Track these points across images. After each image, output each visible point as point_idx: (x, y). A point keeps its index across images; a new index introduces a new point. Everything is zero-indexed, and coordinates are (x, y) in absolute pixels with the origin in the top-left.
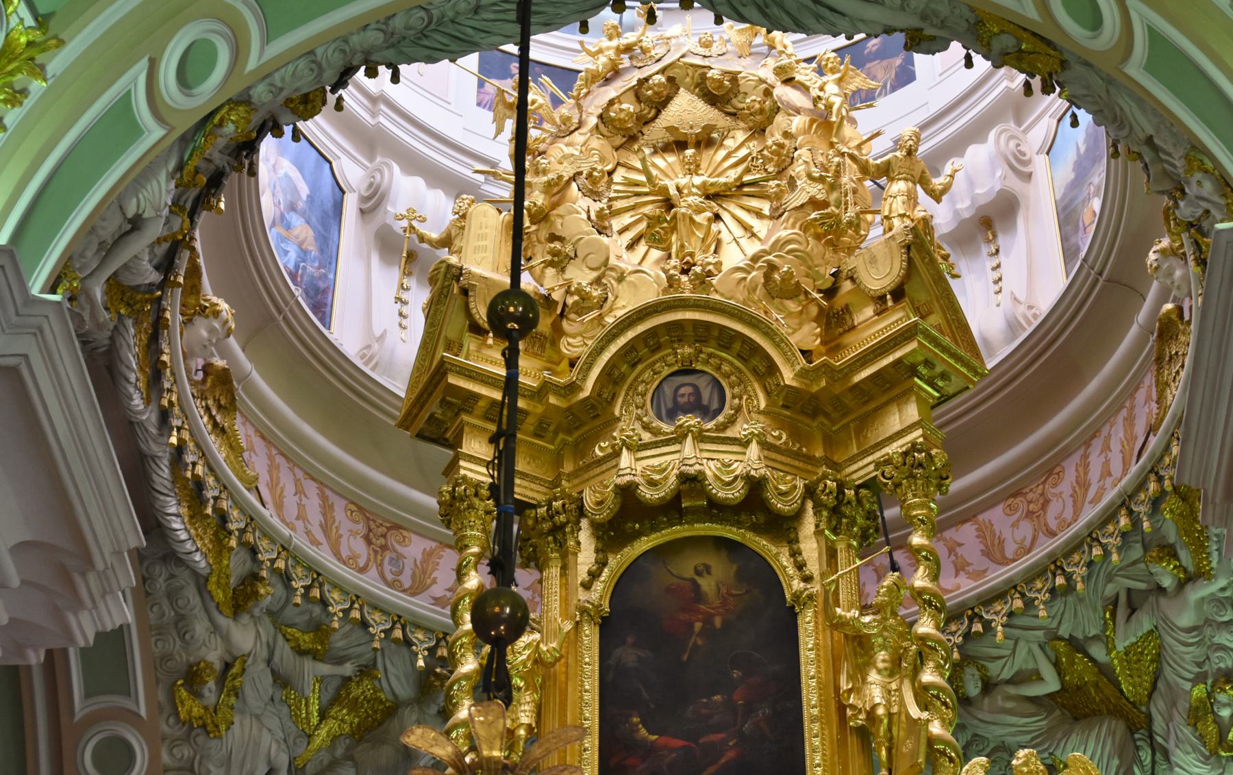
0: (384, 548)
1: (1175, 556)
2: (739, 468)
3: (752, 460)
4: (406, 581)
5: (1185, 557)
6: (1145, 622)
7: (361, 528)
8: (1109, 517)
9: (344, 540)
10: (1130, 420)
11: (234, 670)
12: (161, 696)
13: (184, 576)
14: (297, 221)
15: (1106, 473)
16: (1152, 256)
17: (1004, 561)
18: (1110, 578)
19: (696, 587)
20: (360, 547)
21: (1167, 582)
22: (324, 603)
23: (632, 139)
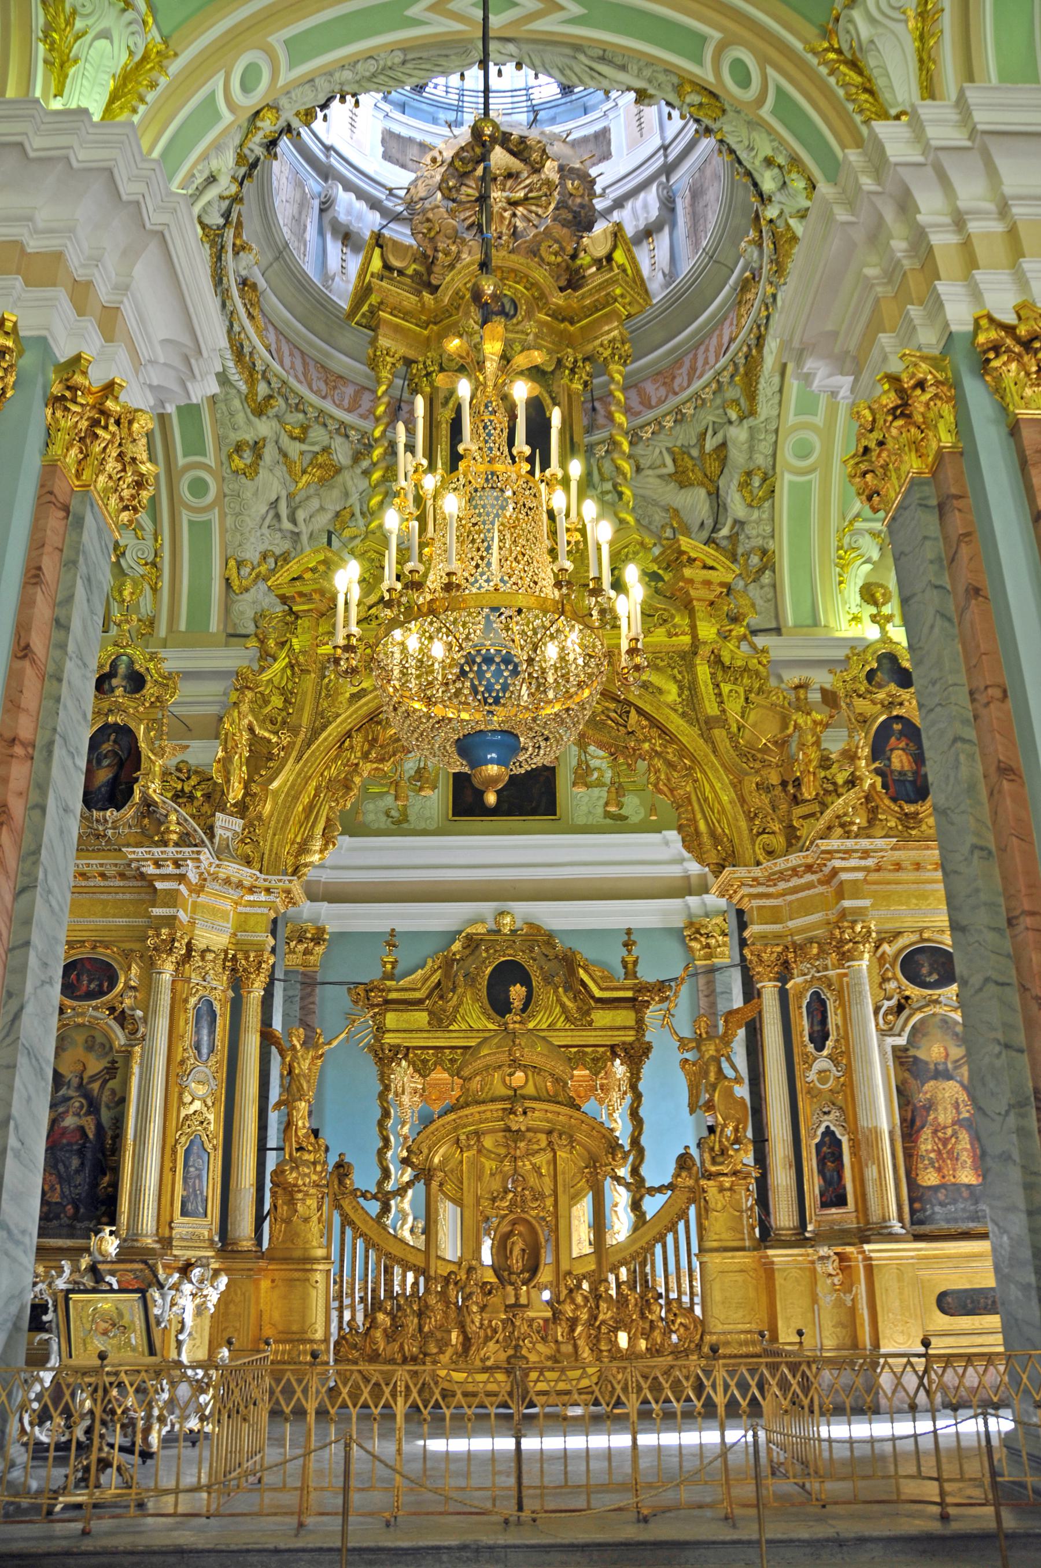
0: (335, 388)
10: (721, 336)
15: (706, 362)
16: (743, 244)
17: (650, 407)
20: (323, 386)
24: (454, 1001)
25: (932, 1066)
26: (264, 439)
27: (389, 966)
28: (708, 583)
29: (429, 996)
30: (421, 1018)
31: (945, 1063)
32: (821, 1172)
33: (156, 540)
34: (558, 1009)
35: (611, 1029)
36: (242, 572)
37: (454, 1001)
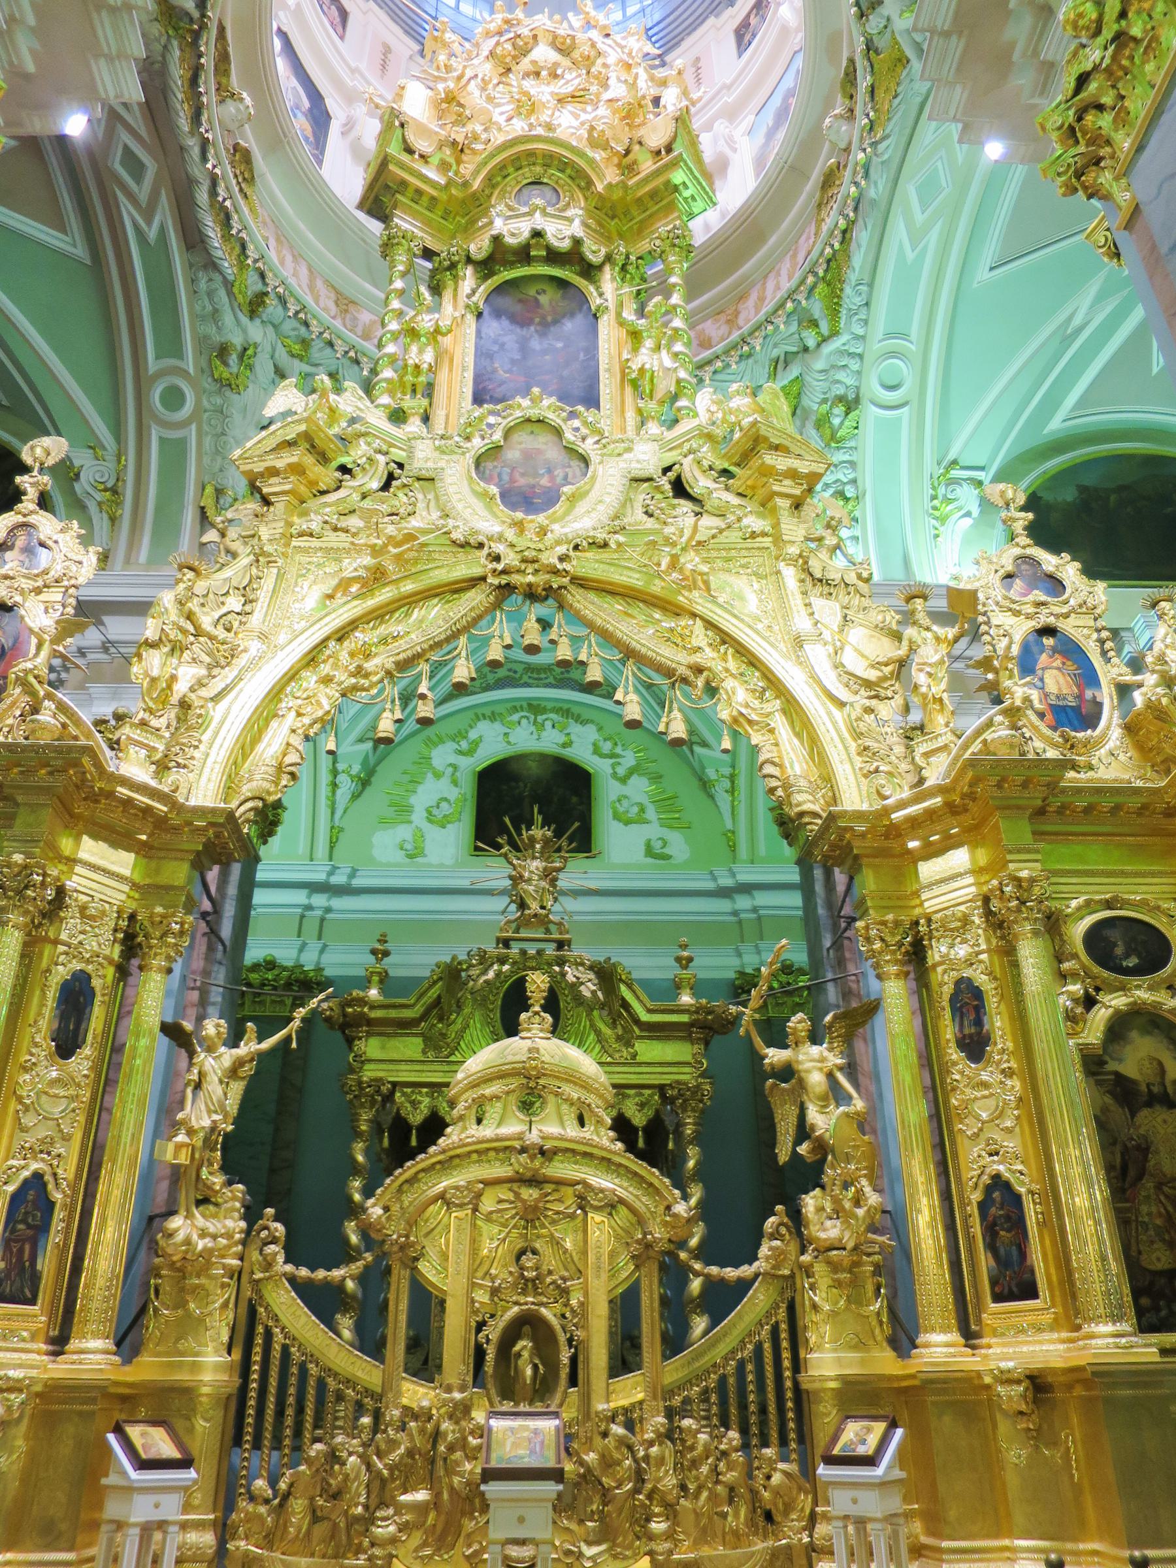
0: (346, 311)
1: (817, 326)
2: (568, 233)
3: (577, 229)
4: (359, 330)
5: (824, 328)
6: (794, 371)
7: (333, 295)
8: (782, 305)
9: (322, 299)
10: (795, 256)
11: (250, 352)
12: (204, 364)
13: (217, 278)
14: (299, 115)
15: (778, 288)
16: (828, 120)
18: (775, 346)
19: (537, 300)
20: (331, 305)
21: (811, 343)
22: (306, 324)
23: (509, 70)
24: (458, 1026)
25: (1144, 1088)
26: (256, 345)
27: (376, 978)
28: (793, 474)
29: (424, 1017)
30: (411, 1047)
31: (1163, 1084)
32: (991, 1247)
33: (119, 461)
34: (592, 1037)
35: (661, 1064)
36: (222, 501)
37: (458, 1026)
